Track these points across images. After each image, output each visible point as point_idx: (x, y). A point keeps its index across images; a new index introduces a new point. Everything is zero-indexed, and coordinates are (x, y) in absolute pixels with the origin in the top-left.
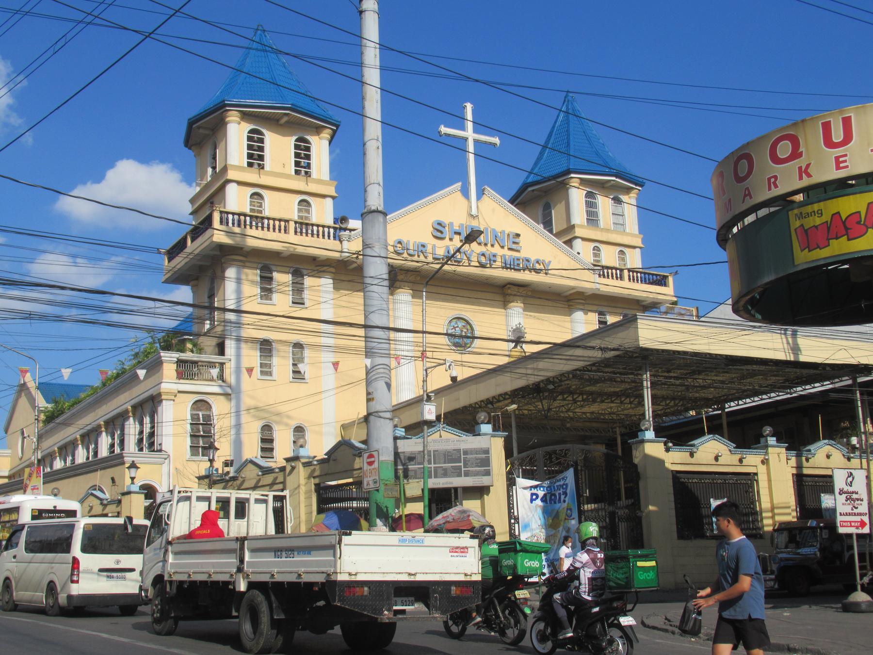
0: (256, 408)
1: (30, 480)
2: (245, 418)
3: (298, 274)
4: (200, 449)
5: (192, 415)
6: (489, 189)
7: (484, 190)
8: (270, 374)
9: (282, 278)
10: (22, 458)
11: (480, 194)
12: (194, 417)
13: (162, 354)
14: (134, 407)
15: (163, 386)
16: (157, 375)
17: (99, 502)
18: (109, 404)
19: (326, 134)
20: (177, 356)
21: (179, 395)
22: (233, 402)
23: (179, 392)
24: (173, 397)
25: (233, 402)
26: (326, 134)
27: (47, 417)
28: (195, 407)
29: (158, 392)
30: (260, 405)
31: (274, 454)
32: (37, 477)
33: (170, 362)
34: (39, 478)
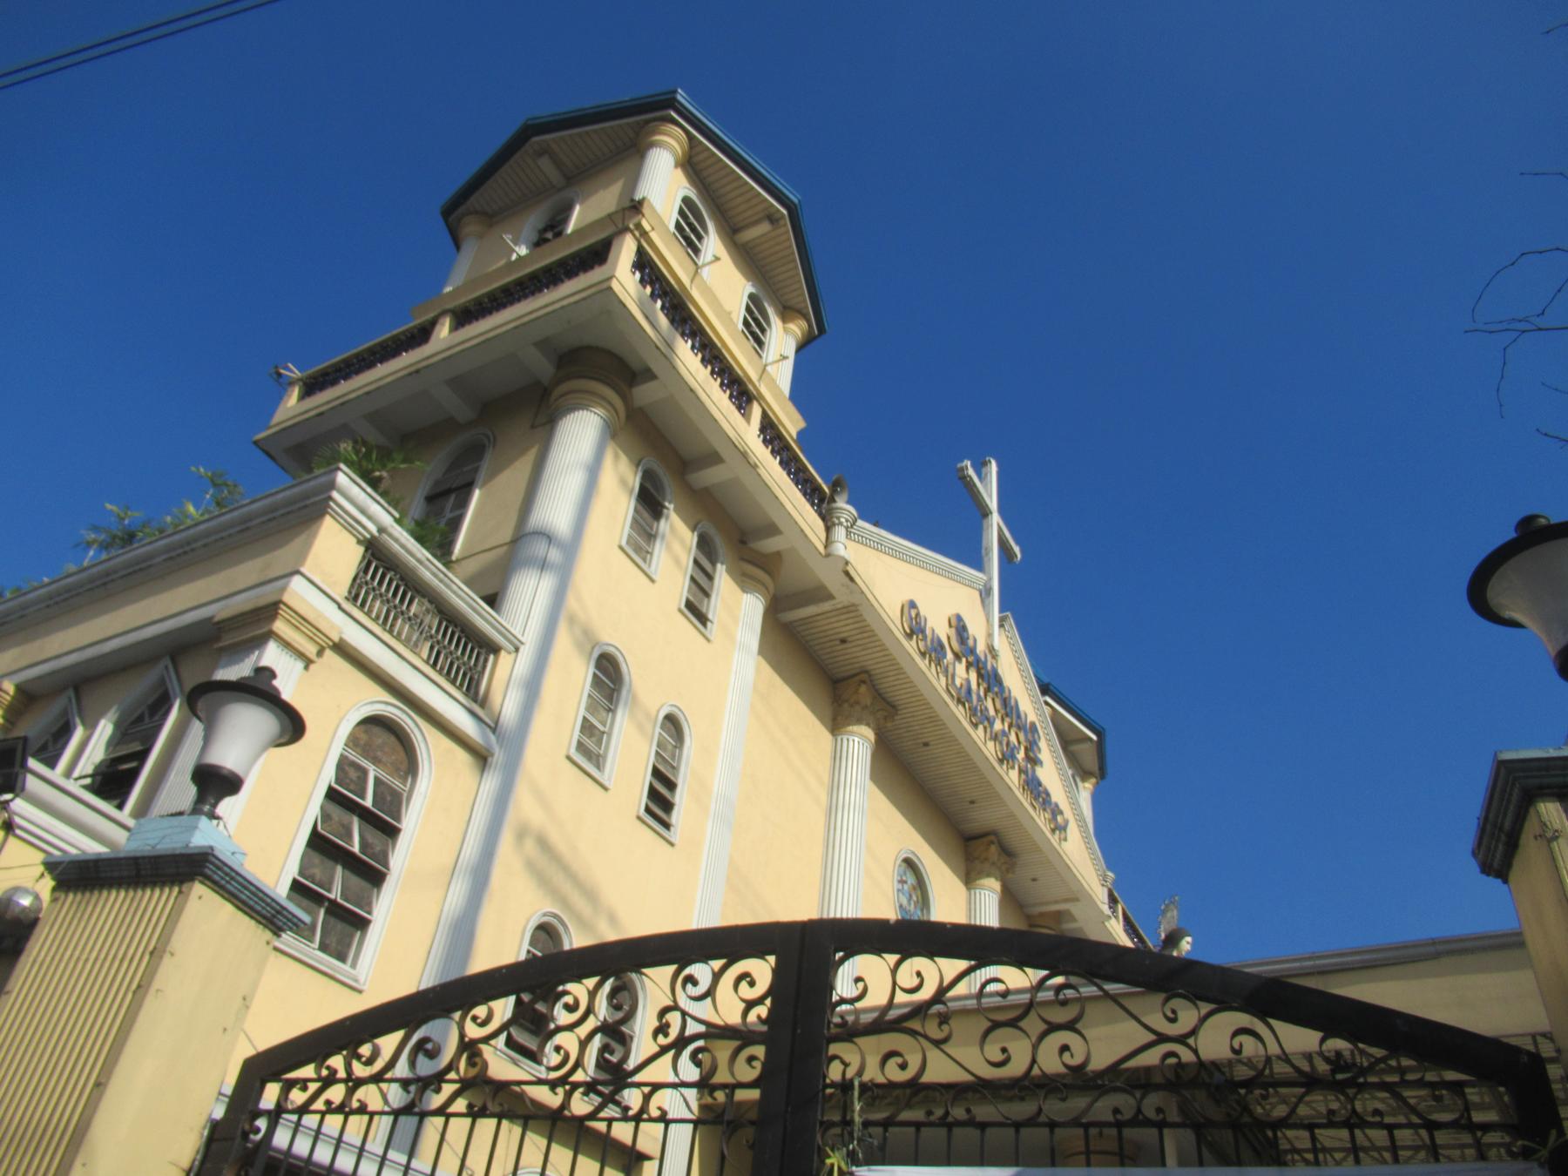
0: (543, 844)
2: (508, 861)
3: (704, 544)
5: (343, 765)
6: (1012, 621)
7: (1006, 617)
8: (597, 760)
11: (1001, 626)
13: (342, 479)
15: (297, 583)
19: (797, 328)
20: (387, 520)
21: (328, 653)
22: (491, 783)
23: (342, 649)
24: (310, 649)
25: (491, 783)
26: (797, 328)
28: (364, 737)
30: (555, 837)
33: (350, 525)
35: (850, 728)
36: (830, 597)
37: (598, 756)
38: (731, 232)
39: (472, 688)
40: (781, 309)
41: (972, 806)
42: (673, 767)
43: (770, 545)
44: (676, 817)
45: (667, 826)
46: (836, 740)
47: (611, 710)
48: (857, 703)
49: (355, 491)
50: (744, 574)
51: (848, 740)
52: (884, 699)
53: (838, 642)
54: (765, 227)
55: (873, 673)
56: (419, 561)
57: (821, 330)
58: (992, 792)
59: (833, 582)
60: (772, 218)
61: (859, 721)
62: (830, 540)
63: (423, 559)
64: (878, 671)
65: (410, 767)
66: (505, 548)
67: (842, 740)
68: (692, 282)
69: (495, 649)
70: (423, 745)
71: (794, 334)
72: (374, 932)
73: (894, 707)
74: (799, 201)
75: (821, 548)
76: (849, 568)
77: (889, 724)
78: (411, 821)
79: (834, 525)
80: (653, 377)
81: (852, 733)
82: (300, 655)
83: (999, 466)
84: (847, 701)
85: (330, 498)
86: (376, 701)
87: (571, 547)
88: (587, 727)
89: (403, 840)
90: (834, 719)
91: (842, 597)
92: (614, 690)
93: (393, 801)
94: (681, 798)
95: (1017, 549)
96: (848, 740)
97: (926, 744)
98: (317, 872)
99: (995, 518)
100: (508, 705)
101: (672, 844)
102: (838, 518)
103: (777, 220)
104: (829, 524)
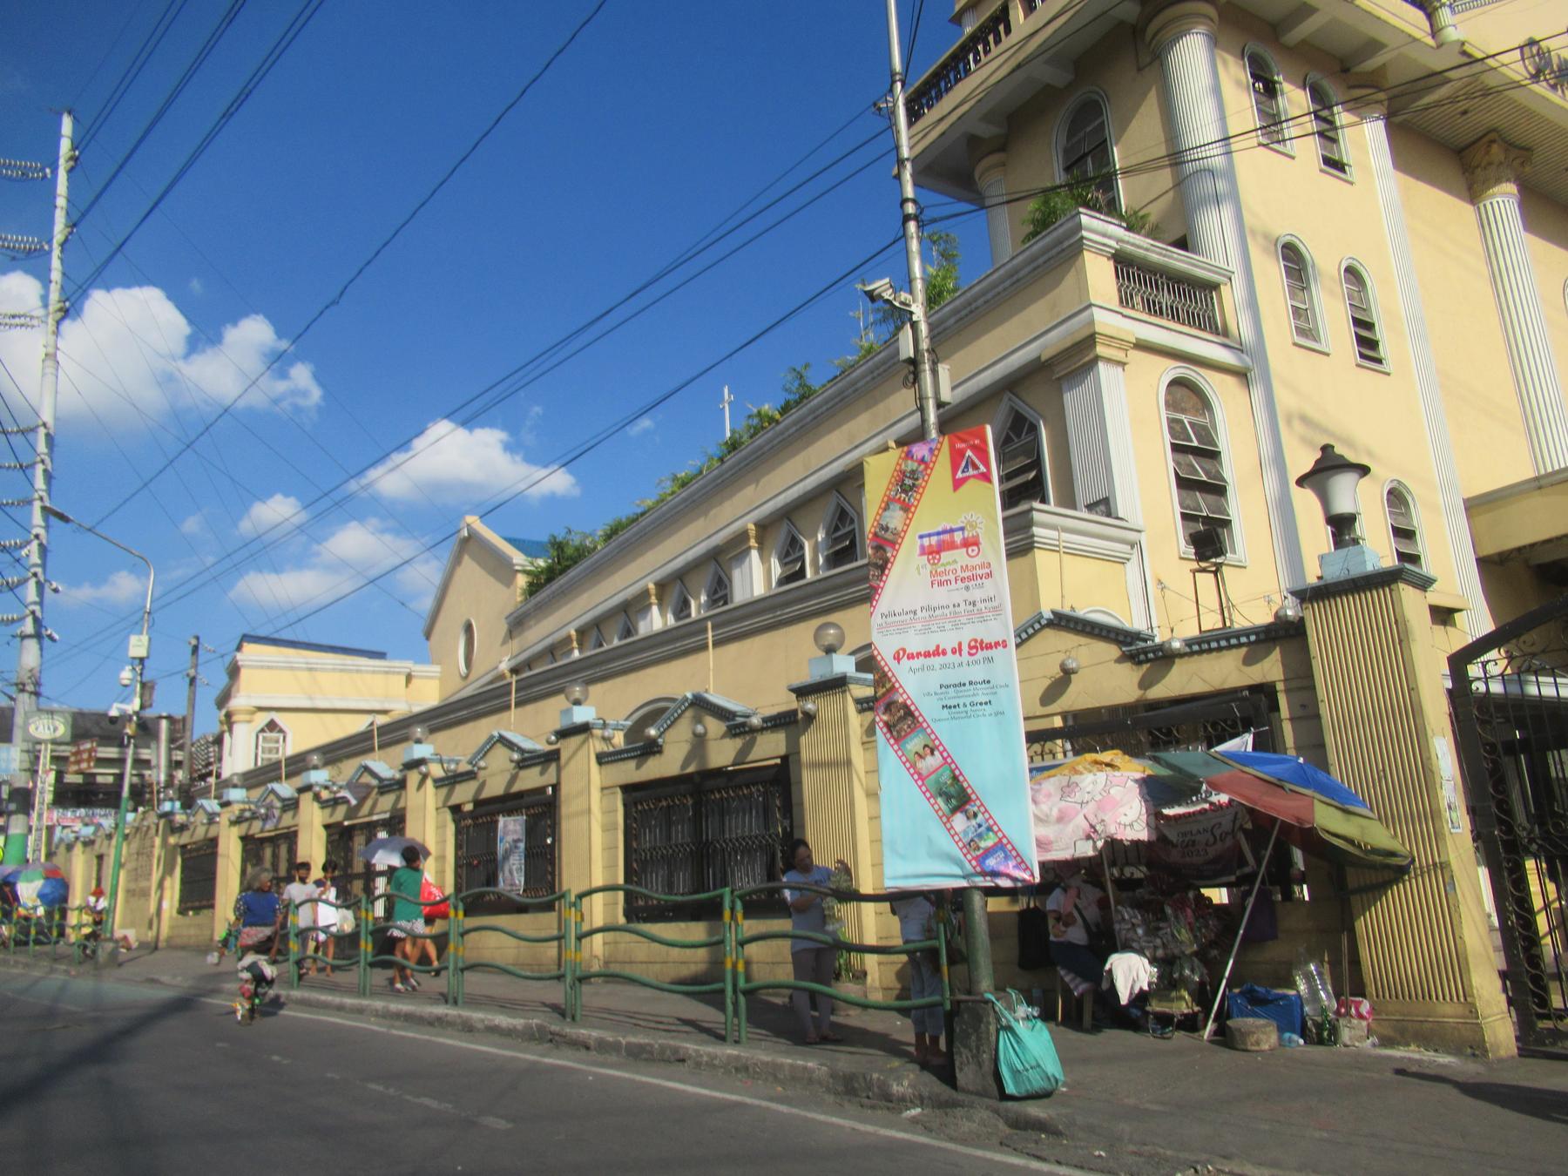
0: (1304, 419)
1: (906, 508)
3: (1318, 95)
9: (1294, 99)
10: (466, 677)
12: (1175, 427)
13: (1084, 220)
14: (662, 586)
16: (1069, 280)
17: (1112, 651)
18: (764, 481)
23: (1143, 346)
25: (1257, 392)
27: (531, 584)
29: (1085, 333)
30: (1311, 412)
32: (957, 484)
34: (973, 487)
35: (1496, 189)
37: (1310, 330)
39: (1220, 331)
42: (1364, 310)
44: (1384, 350)
45: (1379, 361)
46: (1479, 208)
47: (1305, 288)
48: (1490, 164)
49: (1096, 224)
51: (1491, 203)
52: (1515, 147)
56: (1147, 250)
61: (1498, 181)
62: (1435, 28)
63: (1149, 246)
65: (1204, 404)
66: (1171, 194)
67: (1485, 206)
69: (1215, 287)
70: (1207, 386)
72: (1235, 525)
75: (1430, 41)
76: (1467, 48)
78: (1224, 443)
79: (1436, 9)
81: (1494, 196)
84: (1478, 167)
85: (1082, 238)
86: (1171, 370)
87: (1230, 174)
88: (1297, 312)
89: (1224, 457)
90: (1470, 188)
92: (1300, 270)
93: (1206, 434)
94: (1382, 333)
96: (1491, 203)
98: (1188, 502)
100: (1241, 325)
101: (1388, 374)
104: (1430, 10)
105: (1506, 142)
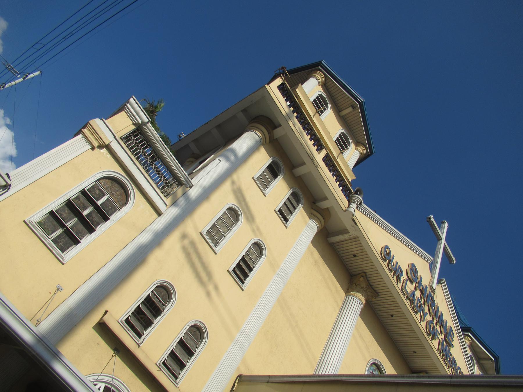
4: (60, 231)
7: (442, 280)
11: (439, 282)
13: (132, 100)
19: (362, 150)
23: (108, 147)
24: (96, 144)
26: (362, 150)
31: (145, 334)
33: (131, 117)
35: (354, 293)
36: (349, 232)
38: (338, 111)
40: (356, 142)
41: (415, 354)
42: (254, 264)
43: (324, 205)
46: (347, 297)
48: (359, 285)
50: (312, 214)
51: (351, 298)
52: (372, 288)
53: (352, 256)
54: (350, 109)
55: (367, 274)
56: (157, 140)
57: (372, 153)
58: (425, 350)
59: (348, 225)
60: (353, 107)
63: (159, 140)
64: (381, 291)
67: (349, 297)
68: (314, 115)
70: (132, 197)
71: (360, 151)
73: (377, 293)
74: (364, 101)
76: (354, 218)
77: (374, 300)
80: (280, 126)
81: (354, 296)
82: (90, 143)
83: (448, 224)
85: (126, 105)
91: (353, 233)
92: (234, 224)
95: (454, 259)
96: (351, 298)
97: (392, 316)
98: (65, 215)
99: (443, 242)
101: (243, 290)
102: (354, 200)
103: (355, 107)
104: (350, 202)
105: (369, 283)
